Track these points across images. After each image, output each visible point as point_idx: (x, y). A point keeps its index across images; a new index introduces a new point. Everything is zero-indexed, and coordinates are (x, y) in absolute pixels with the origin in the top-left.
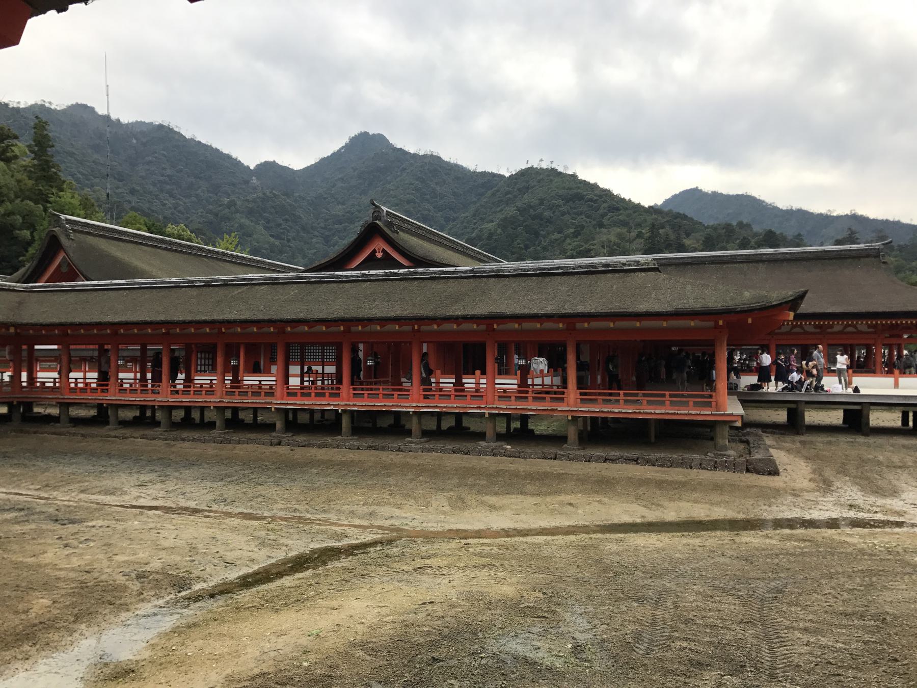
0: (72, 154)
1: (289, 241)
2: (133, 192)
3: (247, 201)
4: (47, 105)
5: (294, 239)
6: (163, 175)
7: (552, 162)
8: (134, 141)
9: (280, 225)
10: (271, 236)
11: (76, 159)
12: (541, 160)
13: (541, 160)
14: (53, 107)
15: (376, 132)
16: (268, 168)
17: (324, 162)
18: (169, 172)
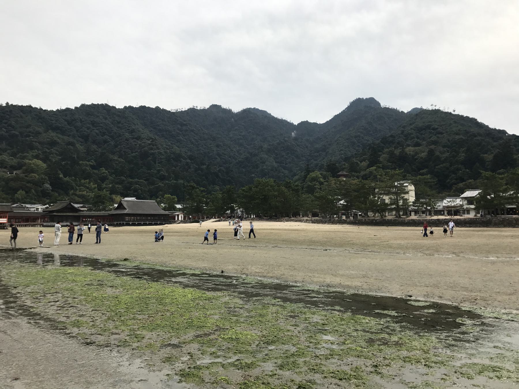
0: (192, 131)
1: (286, 164)
2: (218, 146)
3: (270, 145)
4: (196, 108)
5: (290, 163)
6: (240, 135)
7: (435, 106)
8: (233, 120)
9: (283, 156)
10: (276, 162)
11: (194, 133)
12: (432, 105)
13: (432, 105)
14: (198, 108)
15: (368, 97)
16: (305, 125)
17: (336, 117)
18: (243, 134)
